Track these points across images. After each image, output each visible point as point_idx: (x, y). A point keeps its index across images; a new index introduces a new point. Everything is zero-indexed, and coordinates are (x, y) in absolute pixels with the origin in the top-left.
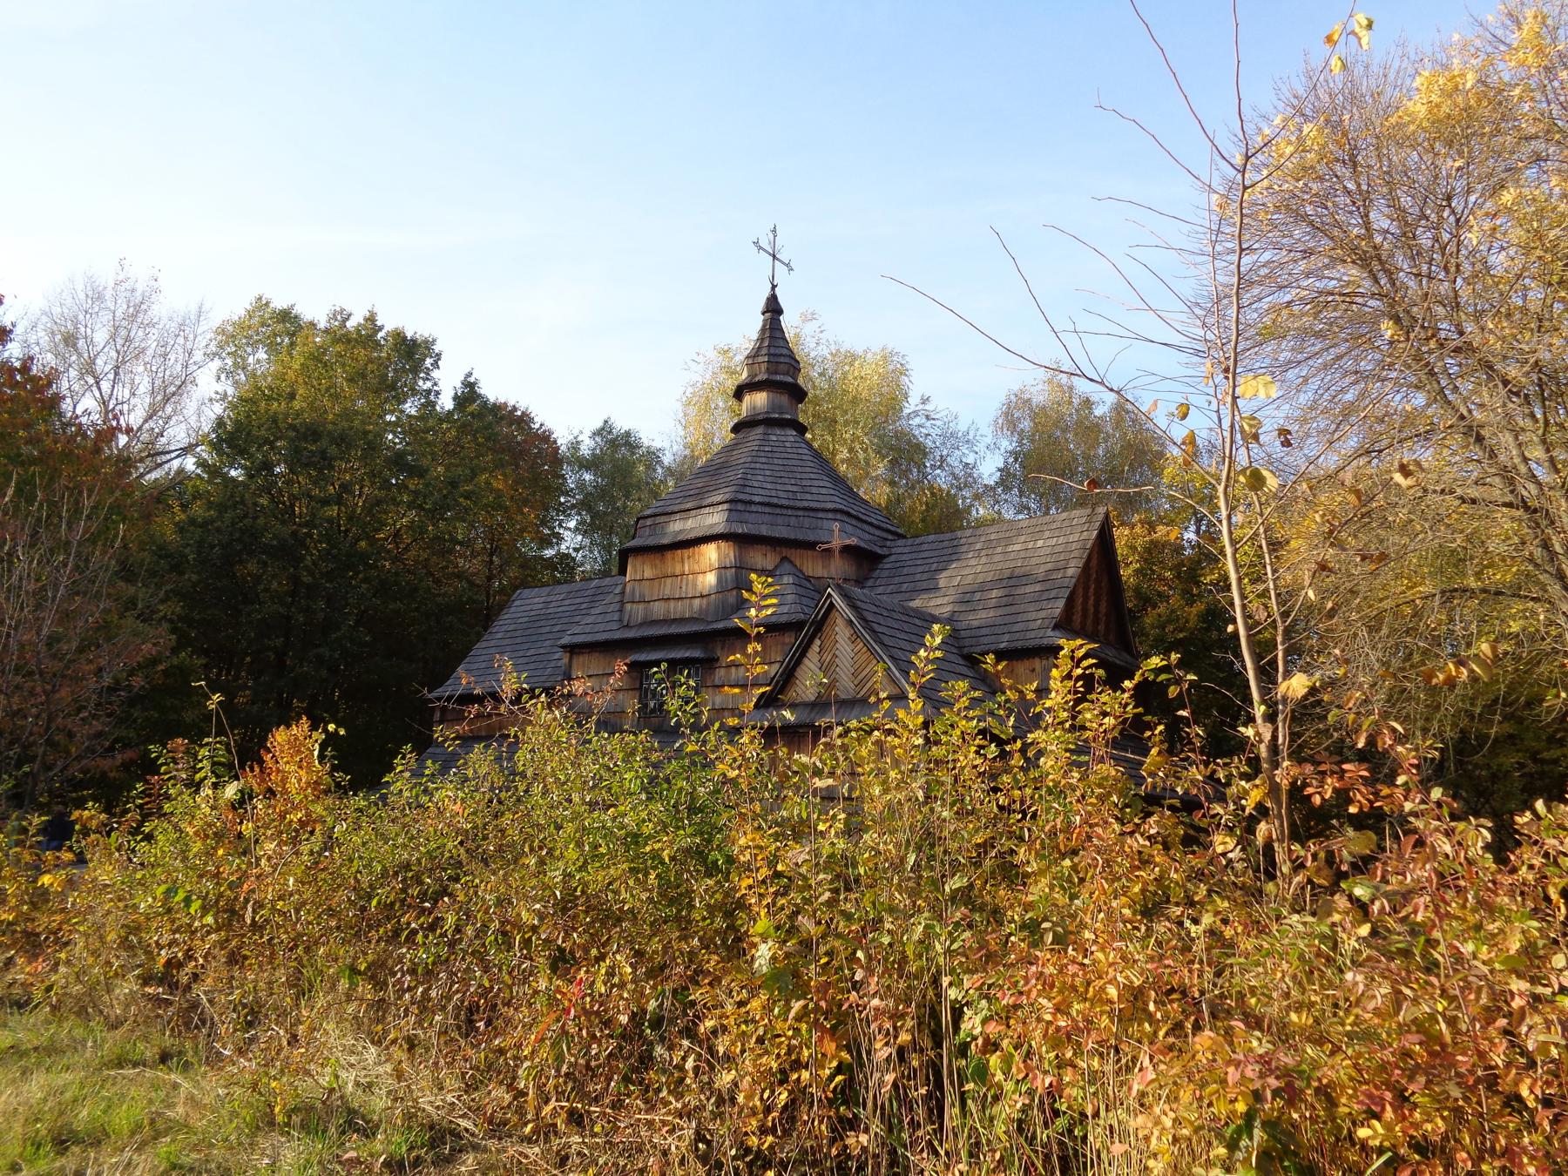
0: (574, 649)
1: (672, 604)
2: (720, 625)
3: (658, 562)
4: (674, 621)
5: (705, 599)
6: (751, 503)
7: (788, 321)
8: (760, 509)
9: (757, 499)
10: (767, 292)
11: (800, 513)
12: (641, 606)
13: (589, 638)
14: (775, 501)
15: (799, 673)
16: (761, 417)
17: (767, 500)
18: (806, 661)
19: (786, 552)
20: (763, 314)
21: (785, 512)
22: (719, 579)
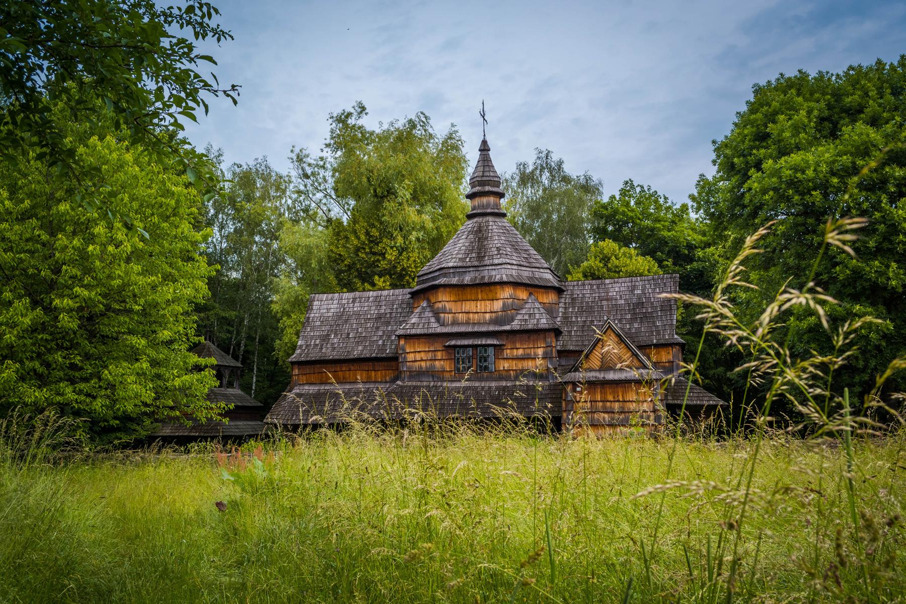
0: (408, 337)
1: (471, 315)
2: (507, 328)
3: (460, 292)
4: (474, 324)
5: (494, 314)
6: (513, 264)
7: (491, 154)
8: (515, 267)
9: (514, 262)
10: (482, 138)
11: (534, 270)
12: (450, 316)
13: (419, 332)
14: (522, 263)
15: (591, 357)
16: (489, 211)
17: (518, 263)
18: (594, 351)
19: (531, 290)
20: (480, 150)
21: (527, 269)
22: (504, 304)
